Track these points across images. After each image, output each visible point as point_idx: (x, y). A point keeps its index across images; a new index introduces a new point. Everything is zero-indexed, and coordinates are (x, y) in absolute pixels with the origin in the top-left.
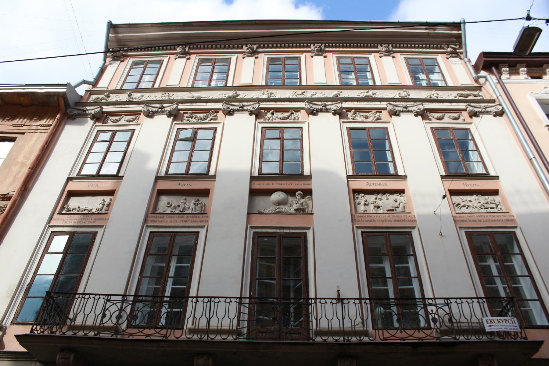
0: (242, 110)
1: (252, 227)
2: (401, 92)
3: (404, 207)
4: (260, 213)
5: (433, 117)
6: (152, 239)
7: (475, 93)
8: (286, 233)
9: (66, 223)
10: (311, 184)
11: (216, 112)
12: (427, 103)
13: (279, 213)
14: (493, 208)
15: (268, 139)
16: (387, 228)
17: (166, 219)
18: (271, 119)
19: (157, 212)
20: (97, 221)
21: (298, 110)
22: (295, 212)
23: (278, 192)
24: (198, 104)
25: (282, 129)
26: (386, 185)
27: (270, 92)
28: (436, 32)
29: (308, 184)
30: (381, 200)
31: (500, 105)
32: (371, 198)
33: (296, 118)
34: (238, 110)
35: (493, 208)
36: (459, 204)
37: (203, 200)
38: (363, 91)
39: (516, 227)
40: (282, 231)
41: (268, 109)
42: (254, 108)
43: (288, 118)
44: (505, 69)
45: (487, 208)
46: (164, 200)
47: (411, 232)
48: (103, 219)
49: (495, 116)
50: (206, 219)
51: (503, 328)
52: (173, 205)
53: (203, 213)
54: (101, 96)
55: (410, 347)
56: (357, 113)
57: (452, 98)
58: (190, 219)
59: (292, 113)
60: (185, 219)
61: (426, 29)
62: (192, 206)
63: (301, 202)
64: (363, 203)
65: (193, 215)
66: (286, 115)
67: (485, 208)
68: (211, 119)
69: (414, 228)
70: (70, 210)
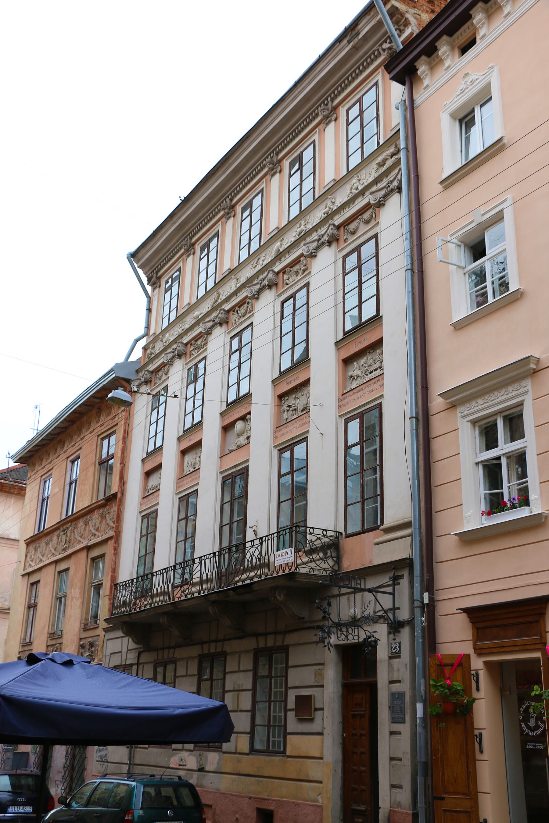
4: (232, 451)
22: (245, 442)
28: (360, 36)
36: (351, 376)
43: (247, 310)
45: (371, 372)
51: (282, 561)
55: (231, 592)
59: (248, 303)
61: (349, 42)
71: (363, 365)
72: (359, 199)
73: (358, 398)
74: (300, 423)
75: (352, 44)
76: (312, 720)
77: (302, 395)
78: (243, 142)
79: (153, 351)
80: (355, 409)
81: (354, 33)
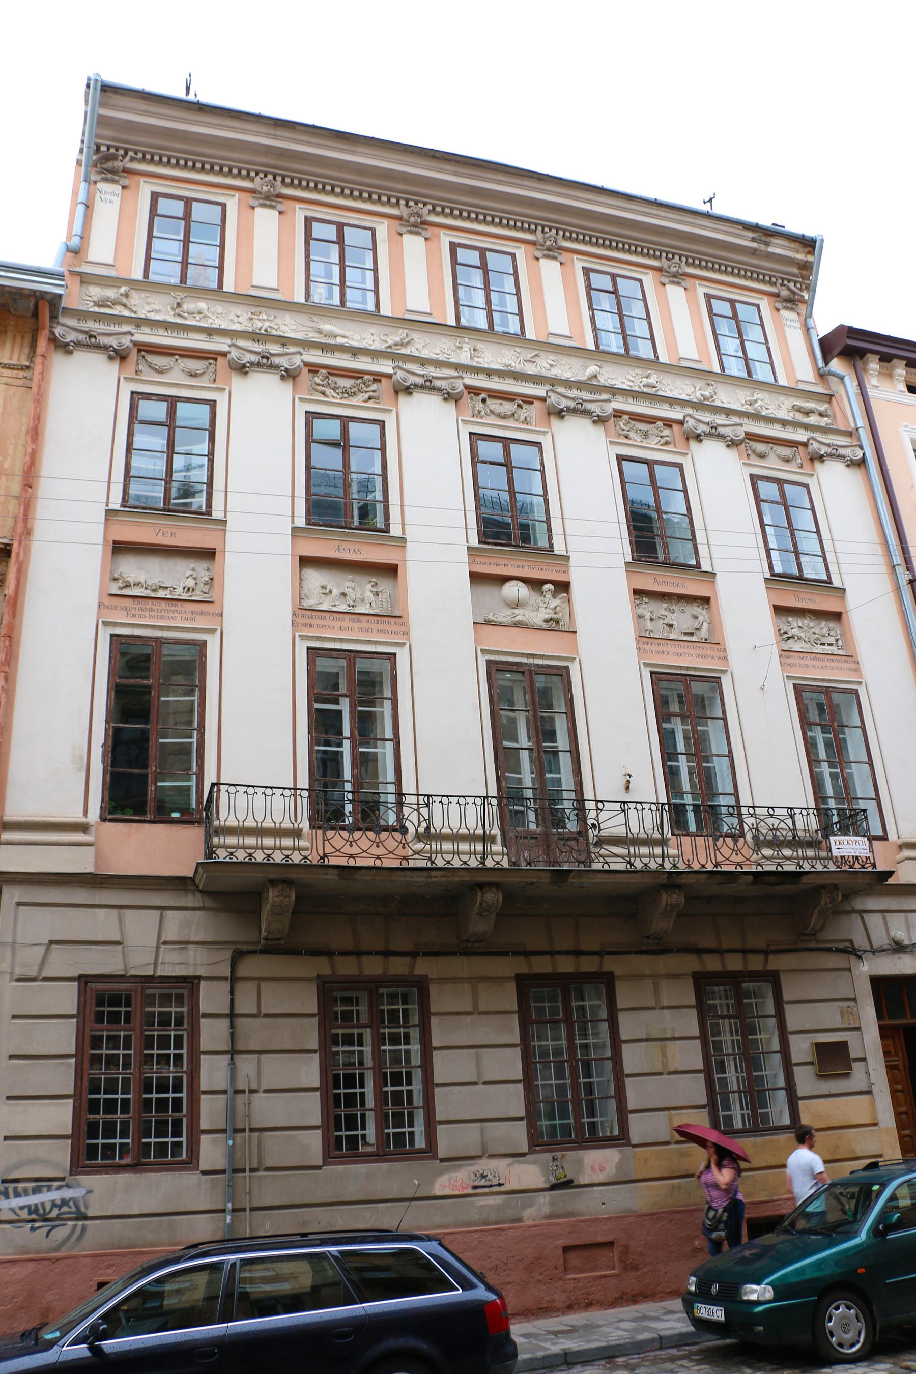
0: (428, 386)
1: (483, 651)
2: (699, 384)
3: (710, 630)
5: (754, 451)
6: (314, 662)
7: (823, 407)
8: (538, 665)
9: (134, 616)
10: (567, 572)
11: (375, 380)
12: (746, 421)
13: (517, 625)
14: (831, 645)
15: (485, 462)
16: (688, 668)
17: (328, 623)
18: (483, 413)
19: (306, 604)
20: (198, 618)
21: (529, 400)
23: (513, 583)
24: (337, 355)
25: (506, 442)
26: (683, 586)
27: (473, 343)
29: (563, 572)
30: (673, 612)
31: (861, 448)
32: (660, 608)
33: (528, 419)
34: (423, 387)
35: (831, 645)
36: (785, 633)
37: (385, 585)
38: (639, 371)
39: (861, 683)
40: (531, 661)
41: (474, 391)
42: (454, 388)
44: (874, 365)
45: (824, 644)
46: (315, 578)
47: (719, 678)
48: (208, 614)
49: (848, 466)
50: (403, 629)
51: (853, 851)
52: (336, 592)
53: (394, 617)
54: (111, 293)
56: (633, 422)
57: (783, 414)
58: (375, 627)
60: (366, 626)
62: (369, 595)
63: (552, 606)
64: (648, 616)
65: (379, 619)
66: (508, 407)
68: (370, 398)
69: (725, 672)
70: (128, 586)
71: (800, 627)
72: (778, 426)
73: (814, 667)
74: (700, 652)
75: (755, 245)
76: (847, 1075)
77: (683, 612)
78: (532, 177)
79: (124, 300)
80: (814, 680)
81: (764, 238)
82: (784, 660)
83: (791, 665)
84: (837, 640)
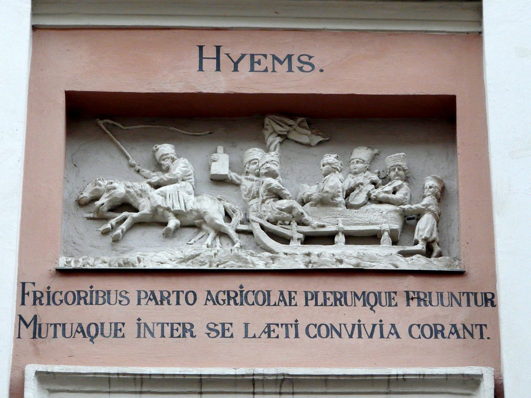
36: (124, 205)
45: (328, 239)
67: (309, 239)
71: (220, 181)
73: (221, 331)
82: (49, 314)
83: (88, 332)
84: (409, 220)
